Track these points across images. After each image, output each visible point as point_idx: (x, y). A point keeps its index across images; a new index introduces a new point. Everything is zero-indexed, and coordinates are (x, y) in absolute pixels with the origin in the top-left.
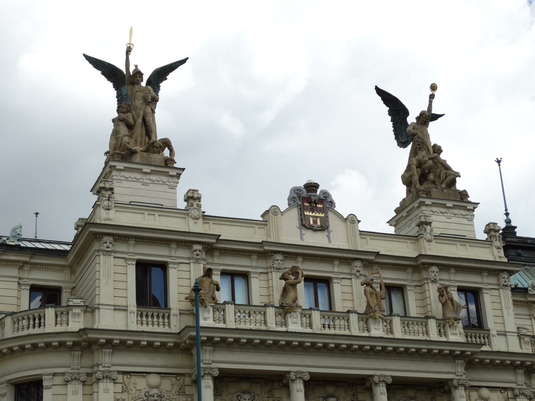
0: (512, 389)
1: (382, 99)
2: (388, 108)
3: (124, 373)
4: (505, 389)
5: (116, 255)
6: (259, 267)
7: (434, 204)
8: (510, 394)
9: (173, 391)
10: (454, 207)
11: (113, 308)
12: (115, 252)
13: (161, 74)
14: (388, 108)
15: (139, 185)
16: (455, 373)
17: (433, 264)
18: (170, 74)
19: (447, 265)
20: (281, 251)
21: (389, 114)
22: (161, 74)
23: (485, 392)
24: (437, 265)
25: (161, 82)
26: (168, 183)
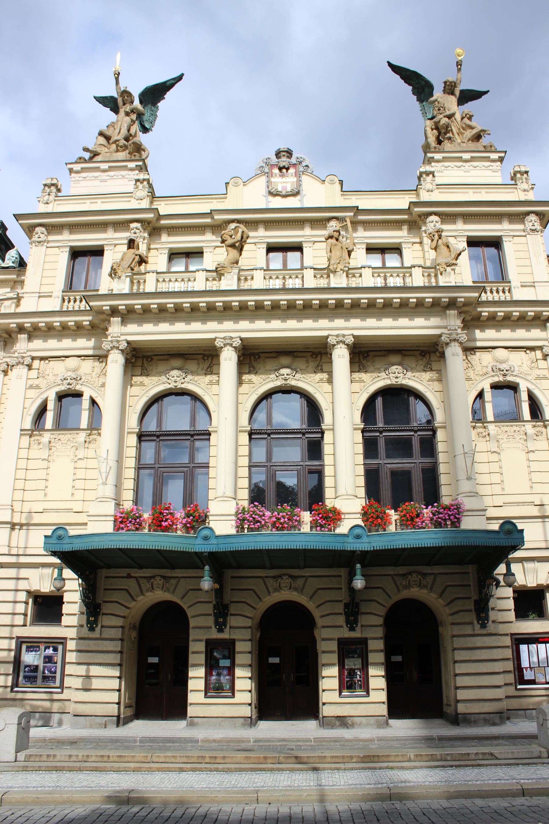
0: (541, 348)
1: (402, 78)
2: (411, 88)
3: (42, 359)
4: (532, 349)
5: (49, 245)
6: (213, 241)
7: (445, 159)
8: (539, 354)
9: (94, 374)
10: (473, 159)
11: (38, 295)
12: (48, 242)
13: (154, 94)
14: (411, 88)
15: (97, 183)
16: (445, 327)
17: (431, 214)
18: (168, 93)
19: (450, 213)
20: (236, 219)
21: (414, 93)
22: (154, 94)
23: (501, 353)
24: (436, 214)
25: (159, 102)
26: (127, 176)
